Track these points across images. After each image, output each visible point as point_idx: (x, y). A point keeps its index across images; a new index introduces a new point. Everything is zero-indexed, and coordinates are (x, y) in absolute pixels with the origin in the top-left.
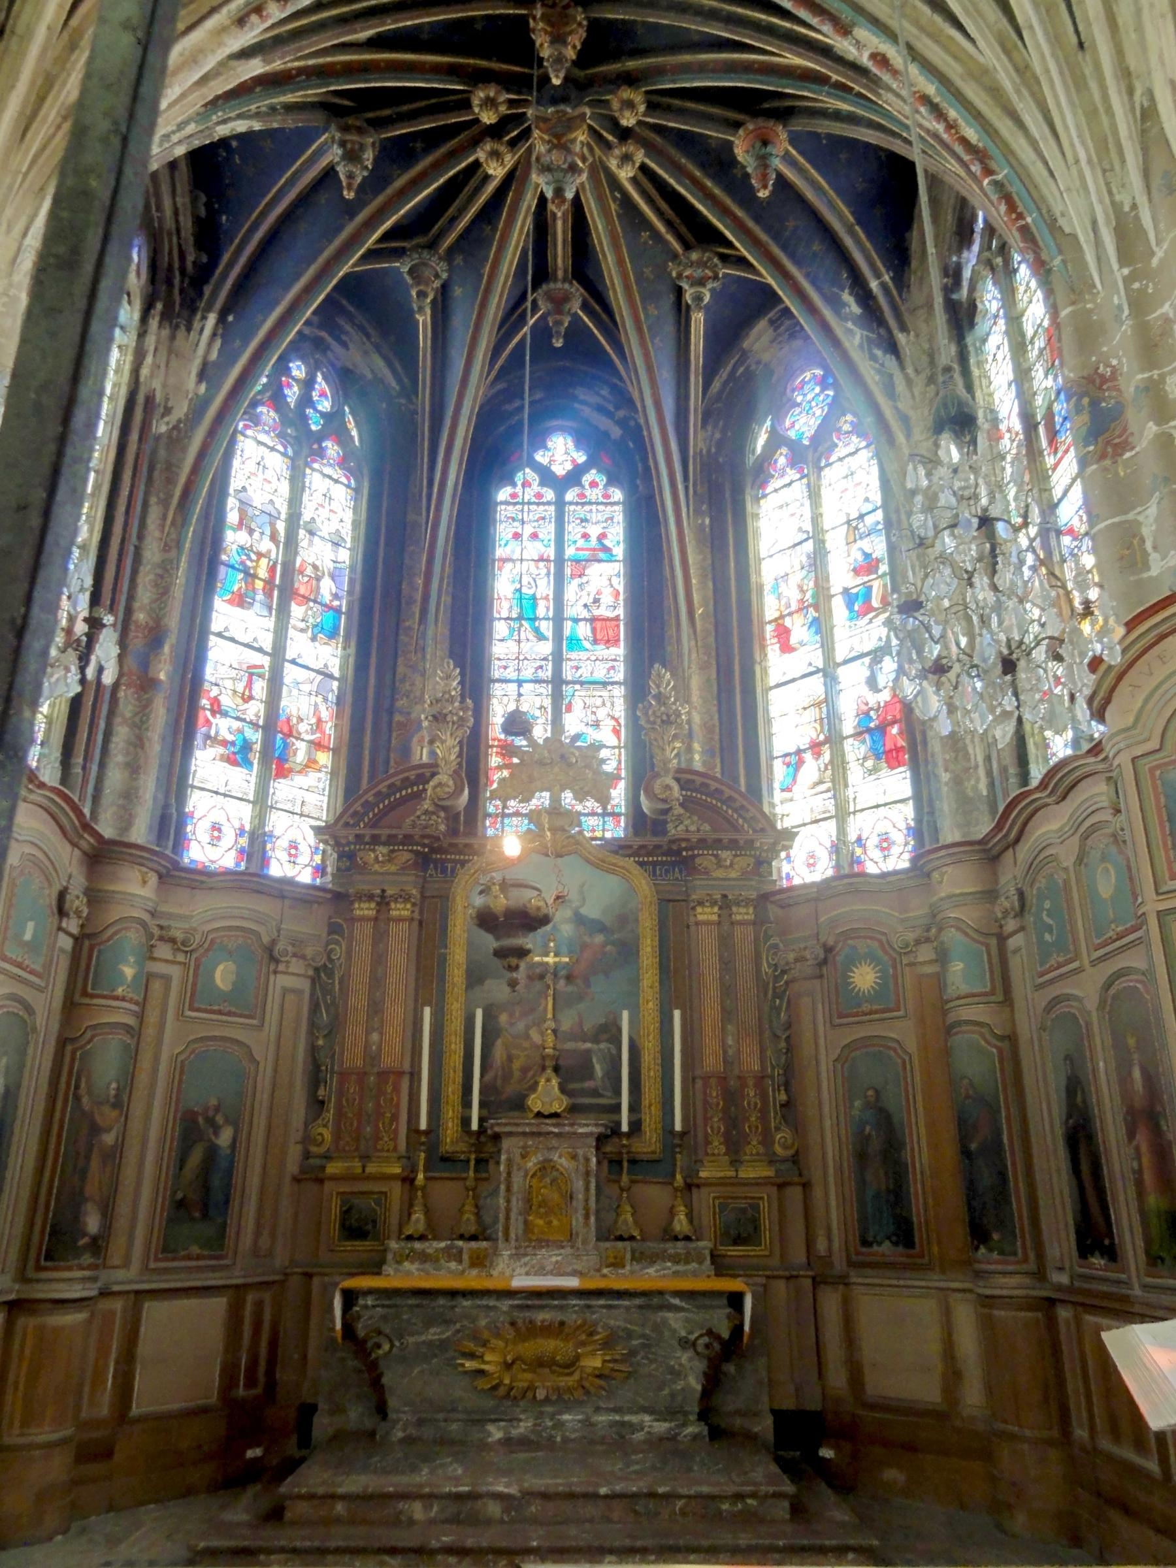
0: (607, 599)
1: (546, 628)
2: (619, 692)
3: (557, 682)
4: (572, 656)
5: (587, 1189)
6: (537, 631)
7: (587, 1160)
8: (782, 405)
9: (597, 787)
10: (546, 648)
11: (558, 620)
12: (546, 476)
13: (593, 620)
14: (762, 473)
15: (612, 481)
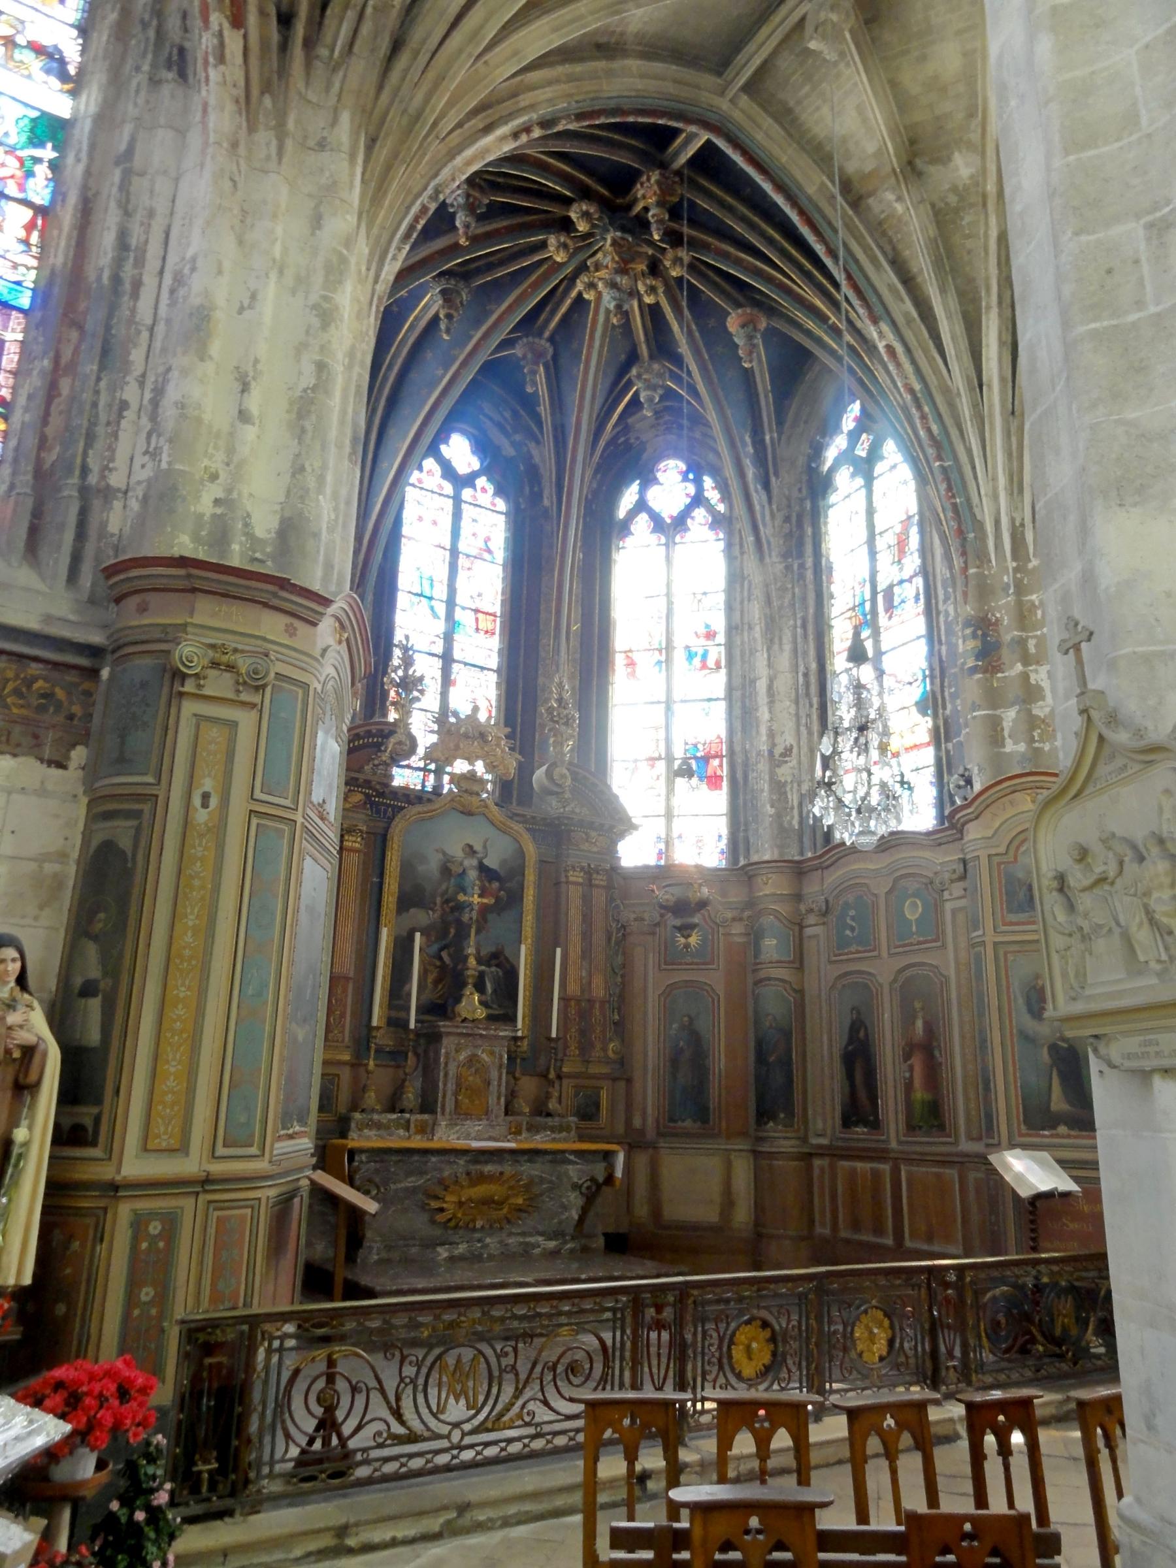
1: (441, 609)
5: (500, 1078)
6: (432, 608)
7: (501, 1057)
8: (648, 479)
10: (440, 626)
11: (451, 603)
12: (448, 471)
14: (624, 528)
15: (500, 491)
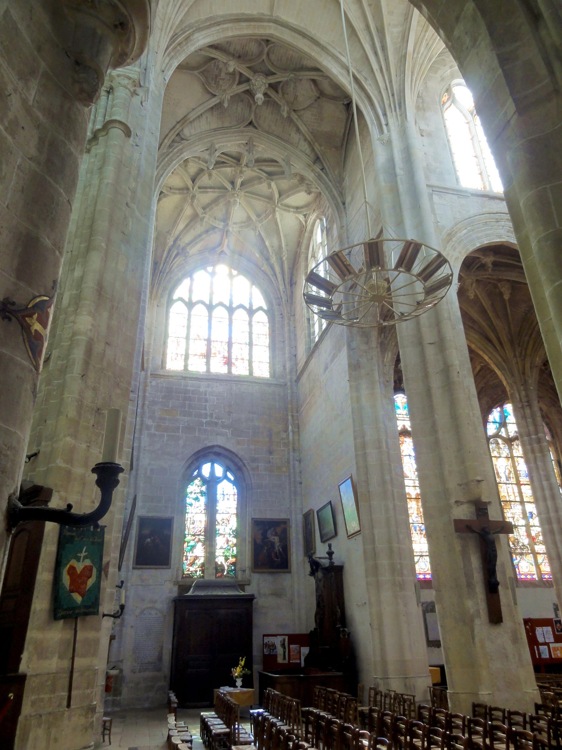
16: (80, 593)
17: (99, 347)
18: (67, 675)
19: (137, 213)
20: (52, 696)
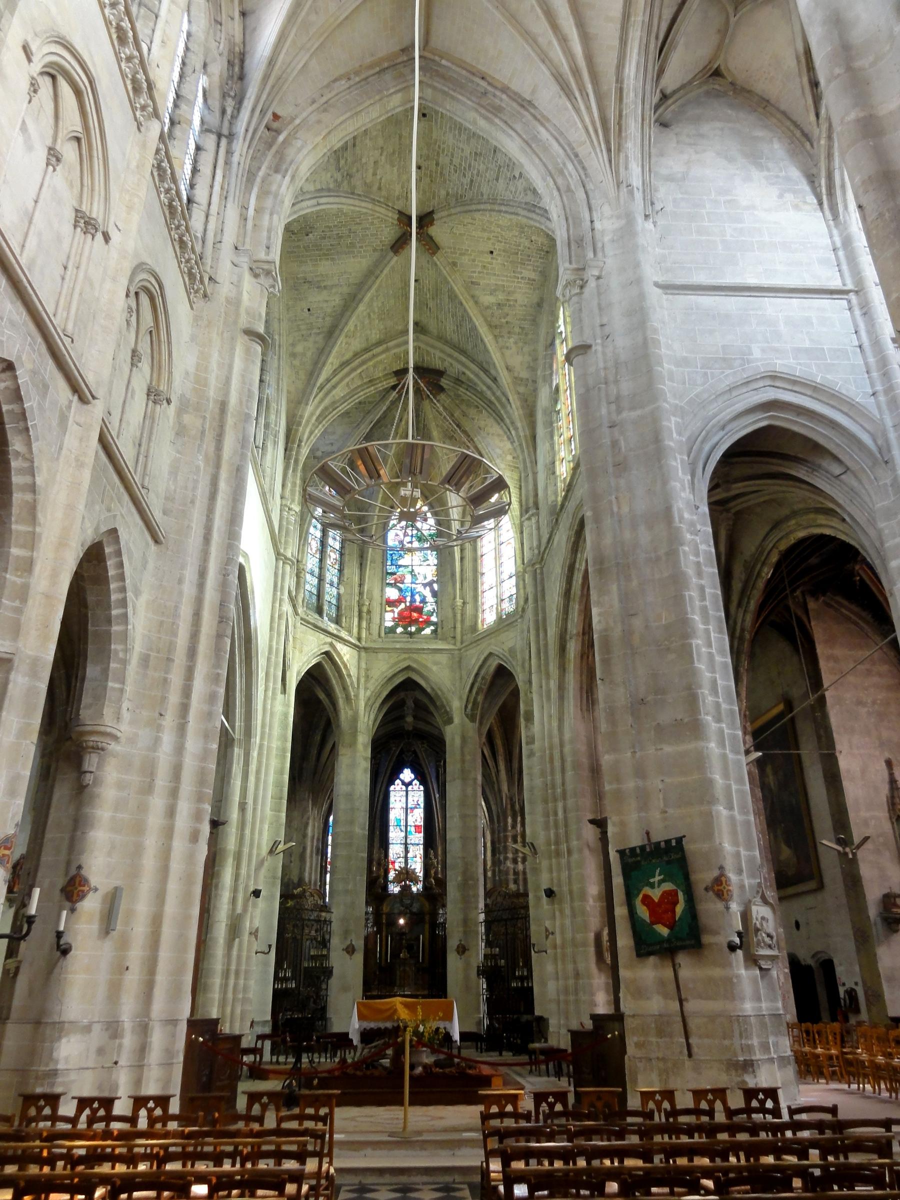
0: (419, 820)
1: (403, 828)
2: (422, 847)
3: (406, 844)
4: (410, 837)
9: (415, 880)
10: (403, 834)
12: (403, 783)
13: (415, 826)
16: (665, 925)
17: (617, 633)
18: (679, 1019)
19: (634, 414)
20: (659, 1040)
